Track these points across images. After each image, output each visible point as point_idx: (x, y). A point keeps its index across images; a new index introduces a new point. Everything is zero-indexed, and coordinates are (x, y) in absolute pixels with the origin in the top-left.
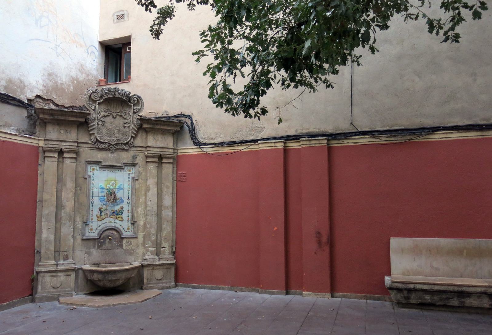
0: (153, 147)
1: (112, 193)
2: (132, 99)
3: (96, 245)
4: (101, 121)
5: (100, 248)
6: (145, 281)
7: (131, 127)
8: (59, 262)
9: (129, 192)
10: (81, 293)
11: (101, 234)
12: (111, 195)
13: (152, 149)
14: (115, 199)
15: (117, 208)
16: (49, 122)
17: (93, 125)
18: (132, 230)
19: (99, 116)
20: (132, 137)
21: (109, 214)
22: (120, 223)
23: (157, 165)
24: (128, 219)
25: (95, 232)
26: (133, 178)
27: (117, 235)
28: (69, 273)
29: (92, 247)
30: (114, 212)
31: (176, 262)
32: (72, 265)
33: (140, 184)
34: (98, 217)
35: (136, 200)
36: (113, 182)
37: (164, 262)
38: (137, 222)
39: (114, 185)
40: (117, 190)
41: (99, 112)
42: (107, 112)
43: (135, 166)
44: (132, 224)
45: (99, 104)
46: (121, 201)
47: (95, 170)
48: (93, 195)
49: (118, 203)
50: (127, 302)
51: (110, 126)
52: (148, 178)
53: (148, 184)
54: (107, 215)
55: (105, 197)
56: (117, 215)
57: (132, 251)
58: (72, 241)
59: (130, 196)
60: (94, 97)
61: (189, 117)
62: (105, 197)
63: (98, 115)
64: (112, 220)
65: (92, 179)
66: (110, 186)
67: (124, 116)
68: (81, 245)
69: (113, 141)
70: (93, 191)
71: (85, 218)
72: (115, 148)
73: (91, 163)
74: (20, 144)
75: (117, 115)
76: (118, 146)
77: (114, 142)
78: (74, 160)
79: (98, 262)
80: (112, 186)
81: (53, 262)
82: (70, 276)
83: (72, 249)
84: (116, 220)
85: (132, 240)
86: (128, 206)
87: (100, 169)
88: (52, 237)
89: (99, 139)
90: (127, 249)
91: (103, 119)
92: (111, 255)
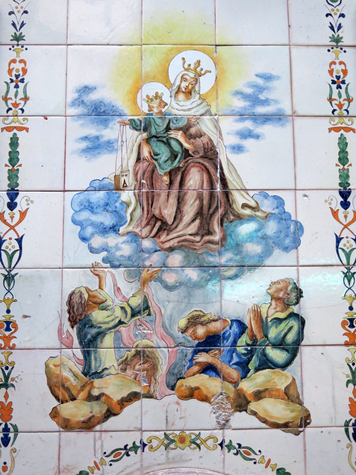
36: (192, 56)
46: (271, 228)
54: (154, 368)
55: (127, 196)
62: (127, 196)
66: (166, 98)
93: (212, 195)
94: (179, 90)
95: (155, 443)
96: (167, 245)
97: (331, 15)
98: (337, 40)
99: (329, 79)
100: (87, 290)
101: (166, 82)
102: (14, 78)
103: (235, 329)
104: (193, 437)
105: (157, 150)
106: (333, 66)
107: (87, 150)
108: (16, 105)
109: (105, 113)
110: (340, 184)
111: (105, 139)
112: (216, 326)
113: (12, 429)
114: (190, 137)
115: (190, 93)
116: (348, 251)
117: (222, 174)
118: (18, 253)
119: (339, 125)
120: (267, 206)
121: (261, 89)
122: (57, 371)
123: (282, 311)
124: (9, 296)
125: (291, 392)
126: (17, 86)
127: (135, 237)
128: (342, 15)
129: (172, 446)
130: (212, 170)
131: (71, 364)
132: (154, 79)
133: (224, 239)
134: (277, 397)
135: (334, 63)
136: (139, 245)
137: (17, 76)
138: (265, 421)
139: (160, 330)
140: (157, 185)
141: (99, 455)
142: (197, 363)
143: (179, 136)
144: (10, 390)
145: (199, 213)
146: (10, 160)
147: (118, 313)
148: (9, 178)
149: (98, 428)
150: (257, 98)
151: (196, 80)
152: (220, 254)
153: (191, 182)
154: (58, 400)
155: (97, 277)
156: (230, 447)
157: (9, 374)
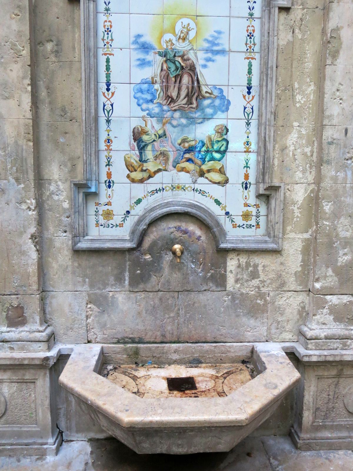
1: (182, 67)
3: (127, 274)
5: (141, 286)
6: (307, 416)
9: (250, 65)
10: (80, 435)
11: (144, 234)
12: (178, 78)
18: (262, 220)
21: (172, 157)
22: (217, 191)
24: (247, 177)
25: (121, 225)
27: (203, 238)
28: (28, 376)
29: (112, 279)
30: (190, 150)
32: (36, 346)
33: (297, 31)
34: (130, 167)
35: (278, 97)
36: (186, 21)
38: (282, 189)
40: (201, 55)
44: (259, 196)
46: (217, 102)
48: (108, 76)
49: (209, 111)
53: (332, 24)
54: (167, 160)
55: (157, 86)
56: (203, 160)
57: (259, 301)
58: (34, 255)
59: (255, 82)
62: (157, 86)
64: (184, 178)
66: (174, 42)
68: (74, 273)
70: (108, 61)
71: (80, 168)
79: (135, 335)
80: (184, 39)
82: (32, 386)
83: (35, 287)
84: (201, 180)
85: (260, 261)
86: (248, 124)
90: (242, 294)
92: (182, 312)
93: (193, 87)
94: (180, 38)
95: (168, 188)
96: (174, 109)
97: (249, 2)
98: (251, 15)
99: (246, 34)
100: (141, 127)
101: (174, 33)
102: (107, 30)
103: (200, 144)
104: (183, 186)
105: (170, 66)
106: (249, 28)
108: (108, 43)
109: (147, 48)
110: (248, 84)
111: (147, 60)
112: (193, 143)
113: (112, 182)
114: (184, 60)
115: (185, 39)
116: (248, 113)
117: (197, 78)
118: (111, 111)
119: (249, 56)
120: (216, 93)
121: (216, 38)
122: (129, 160)
123: (220, 138)
124: (108, 128)
125: (222, 170)
126: (108, 34)
127: (160, 105)
128: (255, 2)
129: (174, 190)
130: (193, 76)
131: (135, 157)
132: (169, 32)
133: (197, 106)
134: (216, 172)
135: (249, 26)
136: (162, 108)
137: (108, 29)
138: (211, 181)
140: (170, 82)
141: (146, 193)
142: (185, 158)
143: (179, 59)
144: (110, 167)
145: (187, 95)
146: (107, 69)
147: (153, 137)
148: (106, 77)
149: (145, 182)
150: (214, 43)
151: (188, 33)
152: (195, 113)
153: (184, 81)
154: (129, 170)
155: (144, 122)
156: (197, 191)
157: (110, 160)
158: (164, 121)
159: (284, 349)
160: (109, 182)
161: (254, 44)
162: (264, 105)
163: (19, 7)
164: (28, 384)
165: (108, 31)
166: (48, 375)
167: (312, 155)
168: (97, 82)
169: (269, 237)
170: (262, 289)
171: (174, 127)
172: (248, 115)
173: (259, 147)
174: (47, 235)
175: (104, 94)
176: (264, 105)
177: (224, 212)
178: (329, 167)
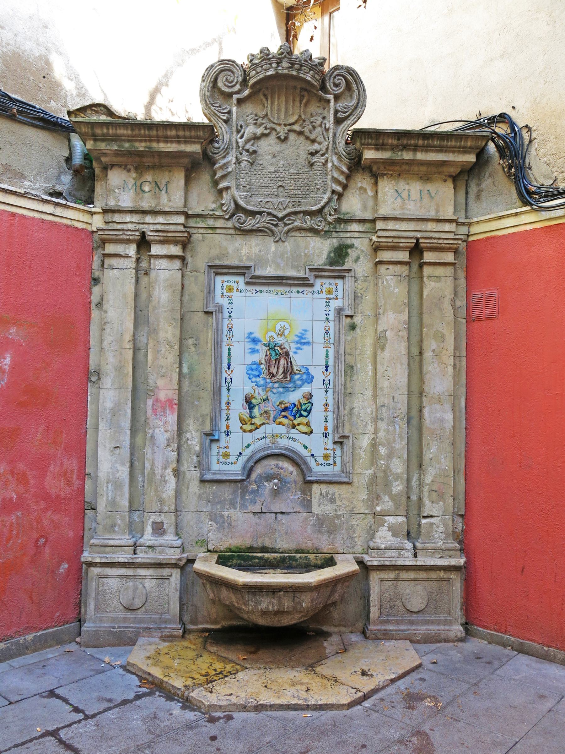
0: (395, 219)
2: (332, 79)
4: (247, 151)
6: (374, 612)
7: (330, 165)
8: (141, 541)
9: (327, 352)
11: (251, 470)
12: (277, 361)
13: (391, 225)
14: (289, 371)
15: (295, 397)
16: (112, 166)
17: (225, 165)
18: (338, 460)
19: (241, 137)
20: (333, 192)
21: (272, 414)
22: (304, 439)
23: (406, 273)
24: (326, 429)
25: (235, 463)
26: (339, 311)
27: (295, 473)
30: (286, 409)
31: (465, 563)
36: (283, 324)
37: (431, 562)
38: (351, 439)
39: (287, 332)
40: (293, 345)
41: (241, 126)
42: (263, 124)
43: (343, 278)
44: (335, 443)
45: (240, 102)
47: (235, 290)
48: (229, 359)
50: (300, 702)
51: (271, 164)
52: (381, 311)
53: (380, 328)
54: (270, 416)
56: (295, 416)
59: (331, 363)
60: (225, 85)
61: (503, 118)
62: (263, 366)
63: (239, 136)
64: (281, 430)
65: (226, 315)
67: (307, 133)
69: (280, 207)
70: (229, 349)
72: (286, 228)
73: (224, 271)
74: (33, 218)
75: (289, 131)
76: (295, 221)
77: (284, 209)
78: (177, 264)
81: (126, 539)
82: (167, 581)
84: (293, 431)
86: (326, 392)
87: (249, 288)
88: (124, 472)
89: (242, 203)
91: (252, 145)
93: (287, 367)
98: (327, 319)
99: (324, 331)
103: (293, 406)
107: (251, 352)
108: (230, 338)
112: (287, 405)
114: (282, 349)
120: (304, 370)
121: (304, 334)
127: (265, 378)
133: (290, 380)
136: (266, 381)
139: (271, 405)
143: (278, 348)
145: (284, 372)
147: (260, 401)
156: (290, 438)
158: (267, 390)
159: (354, 558)
160: (228, 432)
161: (330, 338)
162: (337, 380)
163: (174, 319)
164: (165, 580)
165: (230, 330)
166: (179, 573)
167: (372, 414)
168: (221, 363)
169: (343, 473)
170: (338, 512)
171: (274, 393)
172: (326, 385)
173: (334, 408)
174: (182, 469)
175: (226, 371)
176: (337, 380)
177: (310, 454)
178: (383, 423)
